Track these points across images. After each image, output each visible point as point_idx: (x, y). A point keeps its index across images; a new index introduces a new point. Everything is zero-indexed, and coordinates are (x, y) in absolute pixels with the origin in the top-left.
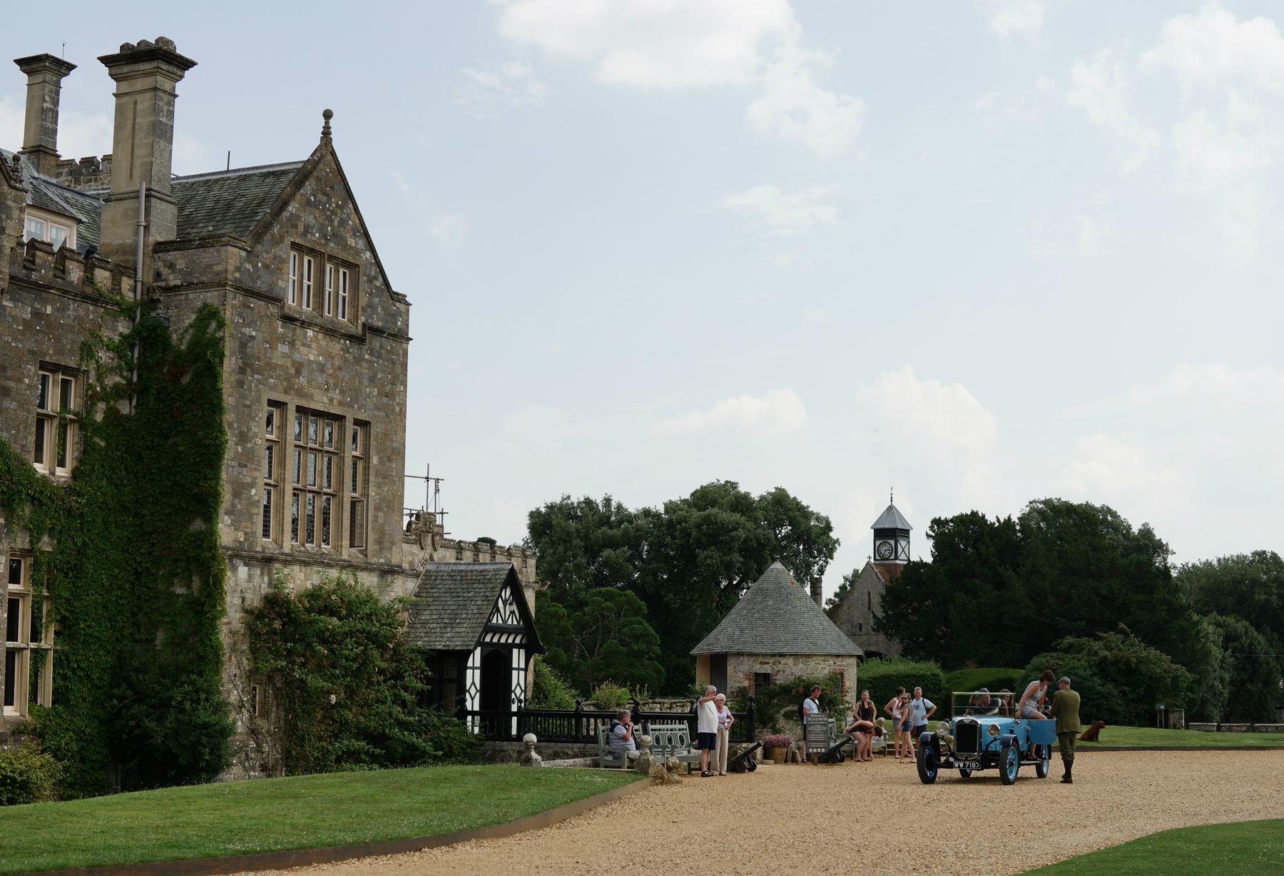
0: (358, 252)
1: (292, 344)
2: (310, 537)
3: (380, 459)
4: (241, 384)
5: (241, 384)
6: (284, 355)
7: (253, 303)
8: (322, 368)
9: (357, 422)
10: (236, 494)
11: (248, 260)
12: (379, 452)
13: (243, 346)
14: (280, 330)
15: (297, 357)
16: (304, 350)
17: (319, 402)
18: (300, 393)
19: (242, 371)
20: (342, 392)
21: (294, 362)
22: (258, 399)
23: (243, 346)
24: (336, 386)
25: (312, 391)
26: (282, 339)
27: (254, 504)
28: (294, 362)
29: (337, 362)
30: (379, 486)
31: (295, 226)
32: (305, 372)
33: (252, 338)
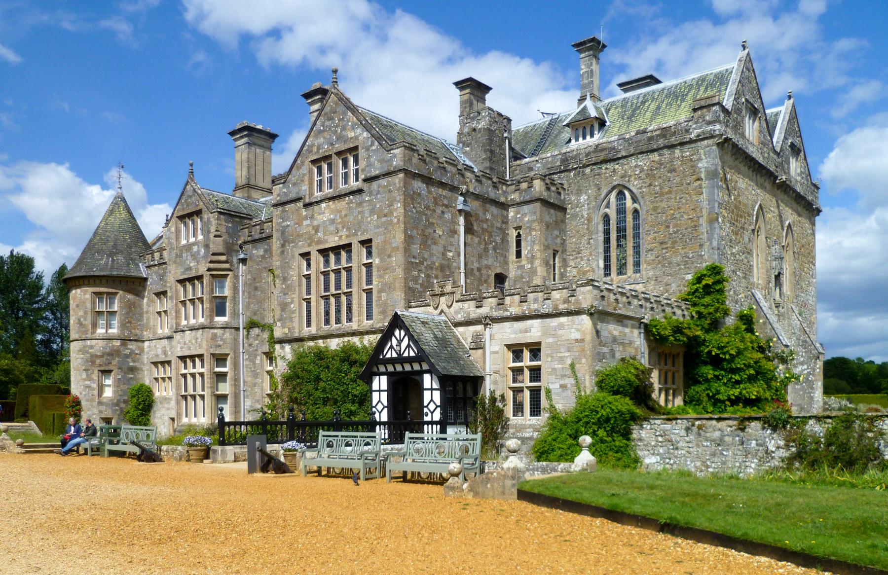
0: (356, 138)
1: (312, 217)
2: (338, 321)
3: (382, 260)
4: (283, 252)
5: (283, 252)
6: (308, 226)
7: (287, 207)
8: (332, 221)
9: (362, 243)
10: (283, 310)
11: (284, 187)
12: (379, 255)
13: (283, 233)
14: (304, 213)
15: (315, 223)
16: (320, 217)
17: (333, 241)
18: (319, 242)
19: (283, 246)
20: (349, 229)
21: (313, 227)
22: (293, 256)
23: (283, 233)
24: (343, 227)
25: (326, 237)
26: (306, 218)
27: (293, 312)
28: (313, 227)
29: (343, 213)
30: (381, 277)
31: (311, 151)
32: (321, 229)
33: (288, 226)
